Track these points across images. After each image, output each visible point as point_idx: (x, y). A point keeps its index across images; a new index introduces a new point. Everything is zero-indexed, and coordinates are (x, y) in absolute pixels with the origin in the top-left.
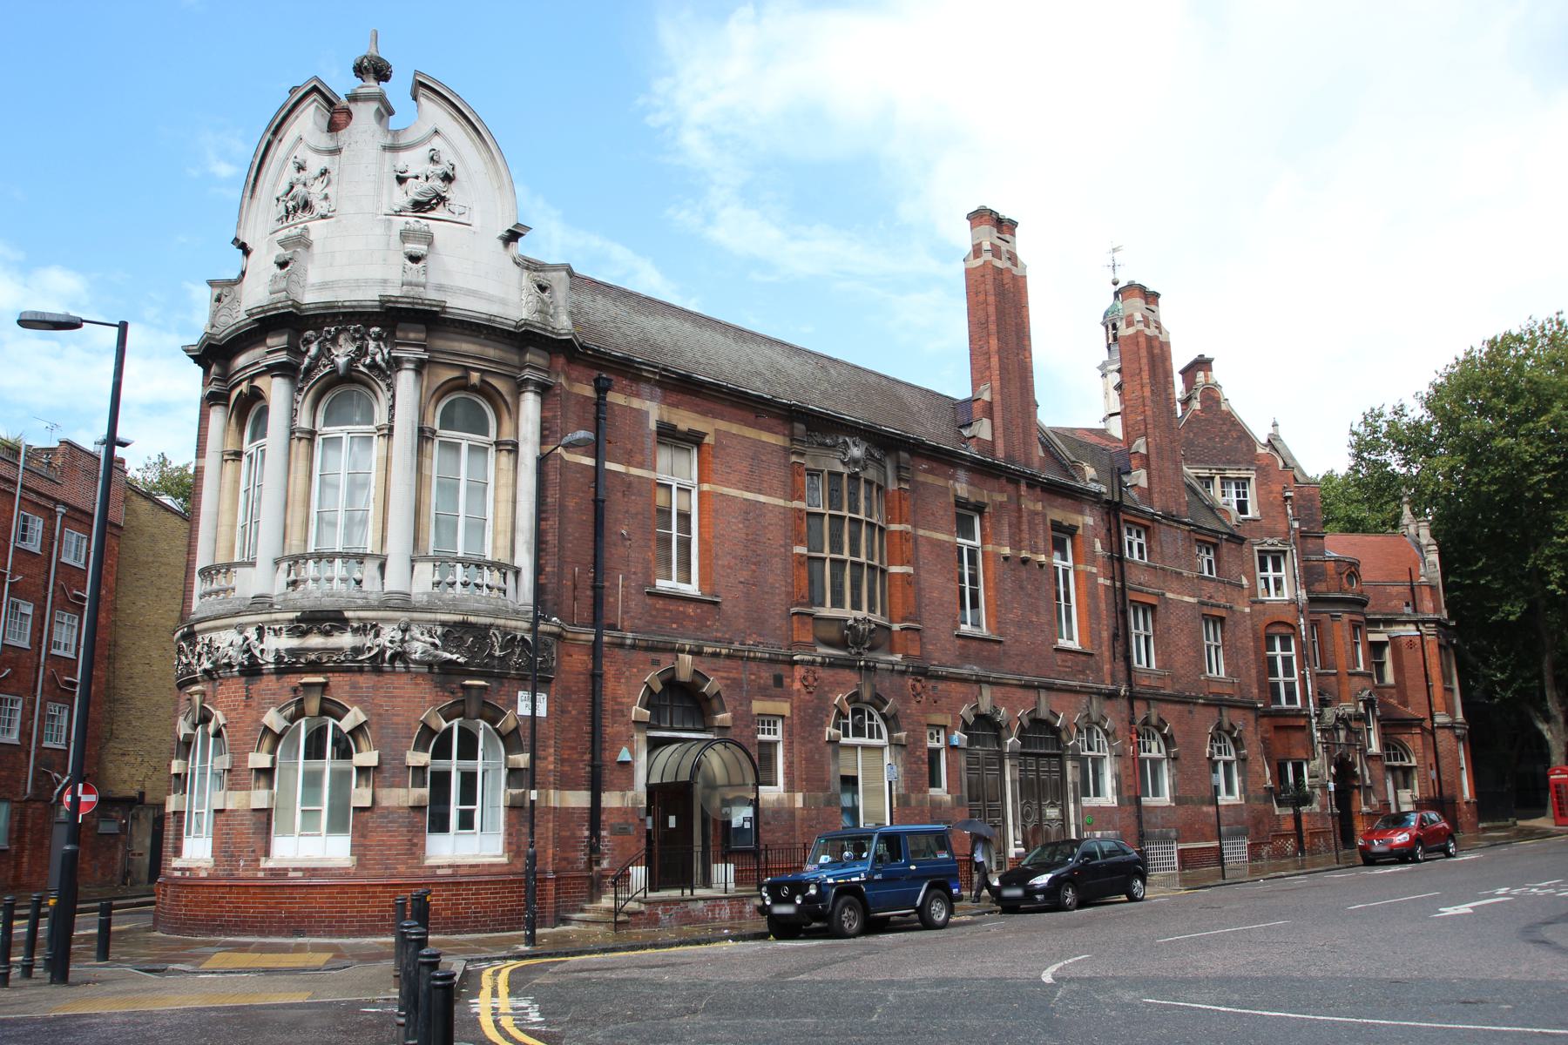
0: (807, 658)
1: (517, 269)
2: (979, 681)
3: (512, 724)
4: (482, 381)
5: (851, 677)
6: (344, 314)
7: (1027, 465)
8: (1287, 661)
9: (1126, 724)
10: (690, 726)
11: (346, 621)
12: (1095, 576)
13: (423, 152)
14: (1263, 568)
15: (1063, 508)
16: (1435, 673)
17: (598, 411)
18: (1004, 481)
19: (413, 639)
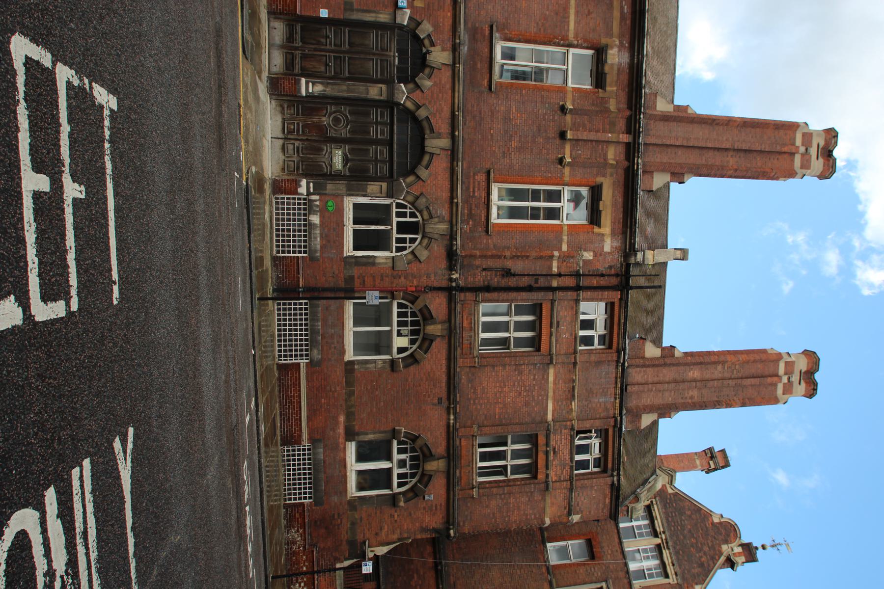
2: (455, 49)
12: (559, 249)
15: (614, 205)
18: (628, 113)
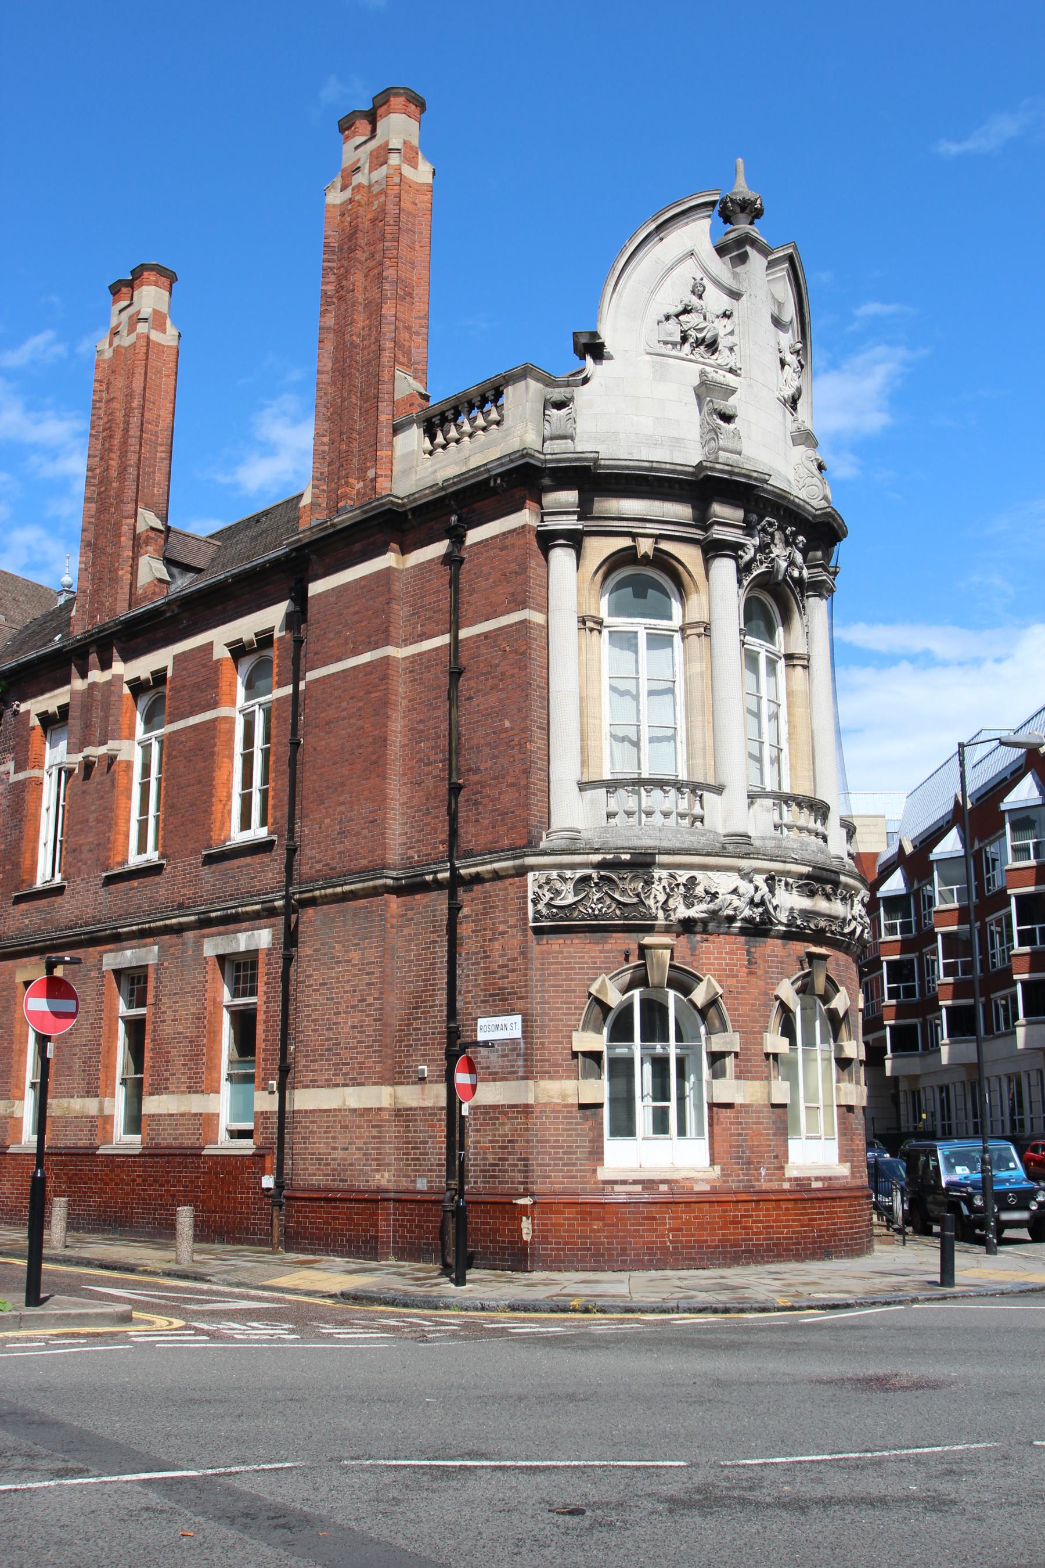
6: (787, 509)
11: (836, 884)
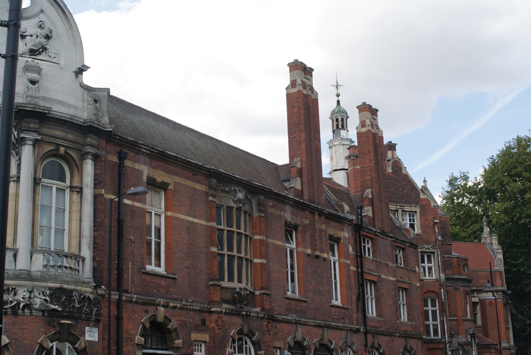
0: (218, 310)
1: (82, 89)
2: (296, 323)
3: (83, 345)
4: (66, 152)
5: (238, 320)
7: (318, 204)
8: (434, 312)
9: (363, 347)
10: (160, 347)
12: (348, 265)
13: (34, 22)
14: (423, 262)
16: (502, 319)
17: (120, 170)
18: (308, 213)
19: (34, 296)
